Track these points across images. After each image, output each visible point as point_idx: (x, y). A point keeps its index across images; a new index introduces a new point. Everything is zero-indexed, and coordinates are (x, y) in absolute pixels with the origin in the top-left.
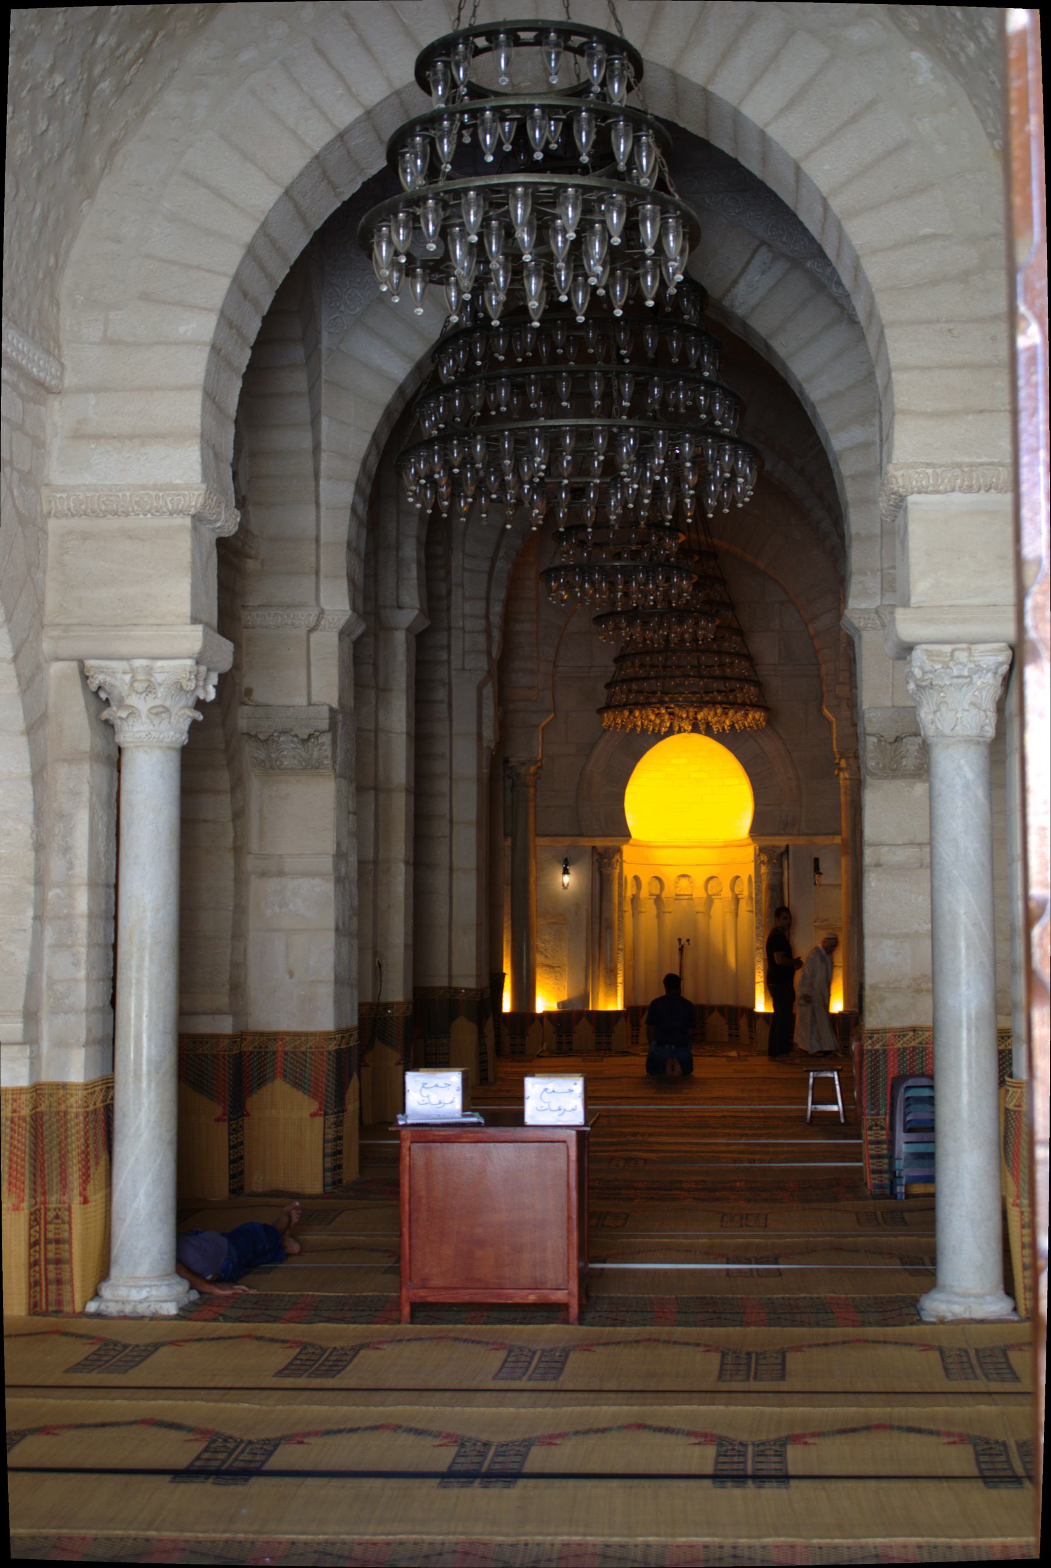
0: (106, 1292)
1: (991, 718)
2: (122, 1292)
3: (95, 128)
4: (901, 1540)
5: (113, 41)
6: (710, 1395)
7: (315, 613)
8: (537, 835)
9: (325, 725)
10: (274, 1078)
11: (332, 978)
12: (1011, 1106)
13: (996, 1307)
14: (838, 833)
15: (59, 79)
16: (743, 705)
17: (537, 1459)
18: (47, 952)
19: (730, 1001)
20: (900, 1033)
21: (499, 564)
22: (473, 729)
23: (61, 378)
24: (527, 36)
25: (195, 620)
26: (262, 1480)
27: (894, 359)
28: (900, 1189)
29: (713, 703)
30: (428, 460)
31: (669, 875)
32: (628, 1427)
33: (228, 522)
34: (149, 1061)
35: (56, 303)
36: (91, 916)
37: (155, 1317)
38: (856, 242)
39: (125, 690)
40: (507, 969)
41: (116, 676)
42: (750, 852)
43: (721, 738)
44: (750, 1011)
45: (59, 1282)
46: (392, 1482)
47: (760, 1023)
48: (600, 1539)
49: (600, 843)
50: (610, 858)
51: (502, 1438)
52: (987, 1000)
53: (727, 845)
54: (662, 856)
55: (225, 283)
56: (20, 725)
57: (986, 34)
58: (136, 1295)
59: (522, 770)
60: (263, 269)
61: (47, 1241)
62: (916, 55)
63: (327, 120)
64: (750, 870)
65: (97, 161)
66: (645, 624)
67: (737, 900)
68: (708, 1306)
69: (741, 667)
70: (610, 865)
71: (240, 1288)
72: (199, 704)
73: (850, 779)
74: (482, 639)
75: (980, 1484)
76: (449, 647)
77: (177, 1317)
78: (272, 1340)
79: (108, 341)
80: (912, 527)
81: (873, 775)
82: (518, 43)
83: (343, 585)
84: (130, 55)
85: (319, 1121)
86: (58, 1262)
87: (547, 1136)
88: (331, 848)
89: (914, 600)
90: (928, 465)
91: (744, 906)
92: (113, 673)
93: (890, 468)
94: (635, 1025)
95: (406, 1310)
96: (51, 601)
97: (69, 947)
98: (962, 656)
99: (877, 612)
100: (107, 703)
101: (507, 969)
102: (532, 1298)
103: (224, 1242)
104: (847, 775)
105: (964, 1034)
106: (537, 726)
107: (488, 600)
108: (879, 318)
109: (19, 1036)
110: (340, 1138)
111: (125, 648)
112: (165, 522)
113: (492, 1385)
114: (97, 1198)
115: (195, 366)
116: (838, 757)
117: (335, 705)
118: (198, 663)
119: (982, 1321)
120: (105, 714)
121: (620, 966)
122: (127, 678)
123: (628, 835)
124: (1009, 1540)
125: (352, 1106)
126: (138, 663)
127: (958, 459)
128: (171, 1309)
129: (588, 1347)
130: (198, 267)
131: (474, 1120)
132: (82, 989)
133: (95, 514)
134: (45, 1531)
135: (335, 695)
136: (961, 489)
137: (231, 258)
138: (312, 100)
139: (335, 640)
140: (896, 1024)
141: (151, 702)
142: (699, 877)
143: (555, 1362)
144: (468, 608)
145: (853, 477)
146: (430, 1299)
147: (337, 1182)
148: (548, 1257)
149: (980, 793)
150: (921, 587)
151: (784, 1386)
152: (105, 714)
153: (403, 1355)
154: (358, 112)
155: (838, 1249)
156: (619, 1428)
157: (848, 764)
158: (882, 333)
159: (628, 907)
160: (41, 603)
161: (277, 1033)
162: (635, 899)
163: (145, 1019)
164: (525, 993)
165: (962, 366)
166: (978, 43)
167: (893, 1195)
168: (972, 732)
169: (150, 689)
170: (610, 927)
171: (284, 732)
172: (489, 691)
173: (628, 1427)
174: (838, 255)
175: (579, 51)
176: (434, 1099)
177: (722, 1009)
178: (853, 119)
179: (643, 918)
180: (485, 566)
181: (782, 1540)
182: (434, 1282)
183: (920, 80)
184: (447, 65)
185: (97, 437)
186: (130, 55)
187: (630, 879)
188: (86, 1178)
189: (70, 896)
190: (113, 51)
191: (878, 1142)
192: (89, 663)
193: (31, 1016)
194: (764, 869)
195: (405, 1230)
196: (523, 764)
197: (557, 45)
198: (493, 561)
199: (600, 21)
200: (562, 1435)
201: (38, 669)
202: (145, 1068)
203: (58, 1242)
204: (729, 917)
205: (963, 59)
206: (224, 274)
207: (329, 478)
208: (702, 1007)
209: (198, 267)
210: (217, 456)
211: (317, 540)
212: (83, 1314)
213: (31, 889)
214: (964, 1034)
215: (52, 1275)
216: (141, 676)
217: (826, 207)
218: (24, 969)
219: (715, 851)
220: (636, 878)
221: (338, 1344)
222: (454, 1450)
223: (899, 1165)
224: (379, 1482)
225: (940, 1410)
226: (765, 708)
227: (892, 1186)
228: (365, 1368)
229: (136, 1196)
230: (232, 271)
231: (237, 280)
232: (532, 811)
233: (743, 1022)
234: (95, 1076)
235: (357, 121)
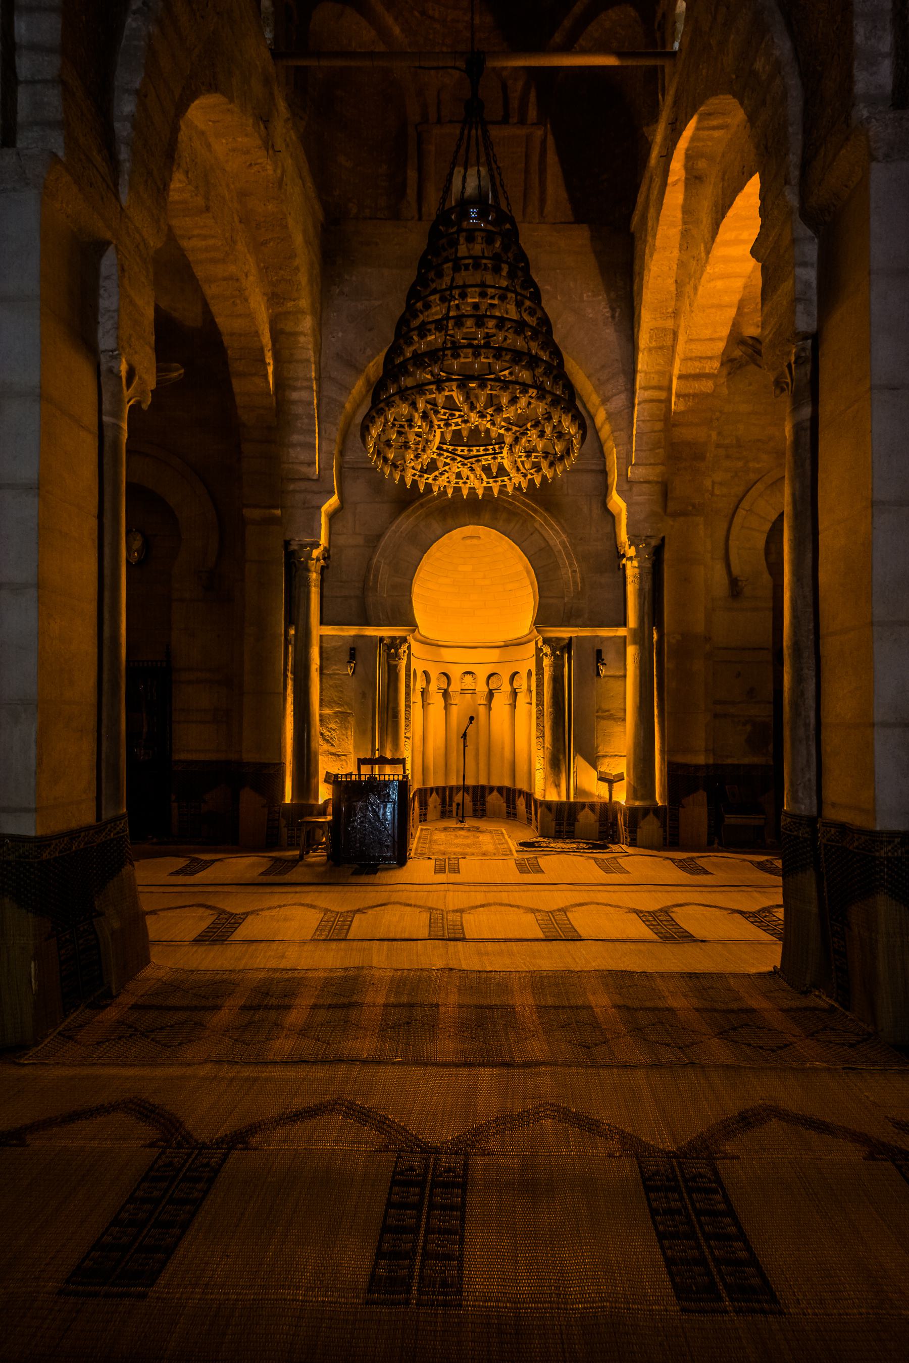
8: (322, 623)
31: (456, 672)
44: (529, 796)
49: (386, 632)
70: (397, 655)
73: (639, 567)
106: (319, 508)
177: (500, 790)
187: (419, 674)
194: (547, 662)
204: (507, 708)
219: (497, 651)
220: (425, 673)
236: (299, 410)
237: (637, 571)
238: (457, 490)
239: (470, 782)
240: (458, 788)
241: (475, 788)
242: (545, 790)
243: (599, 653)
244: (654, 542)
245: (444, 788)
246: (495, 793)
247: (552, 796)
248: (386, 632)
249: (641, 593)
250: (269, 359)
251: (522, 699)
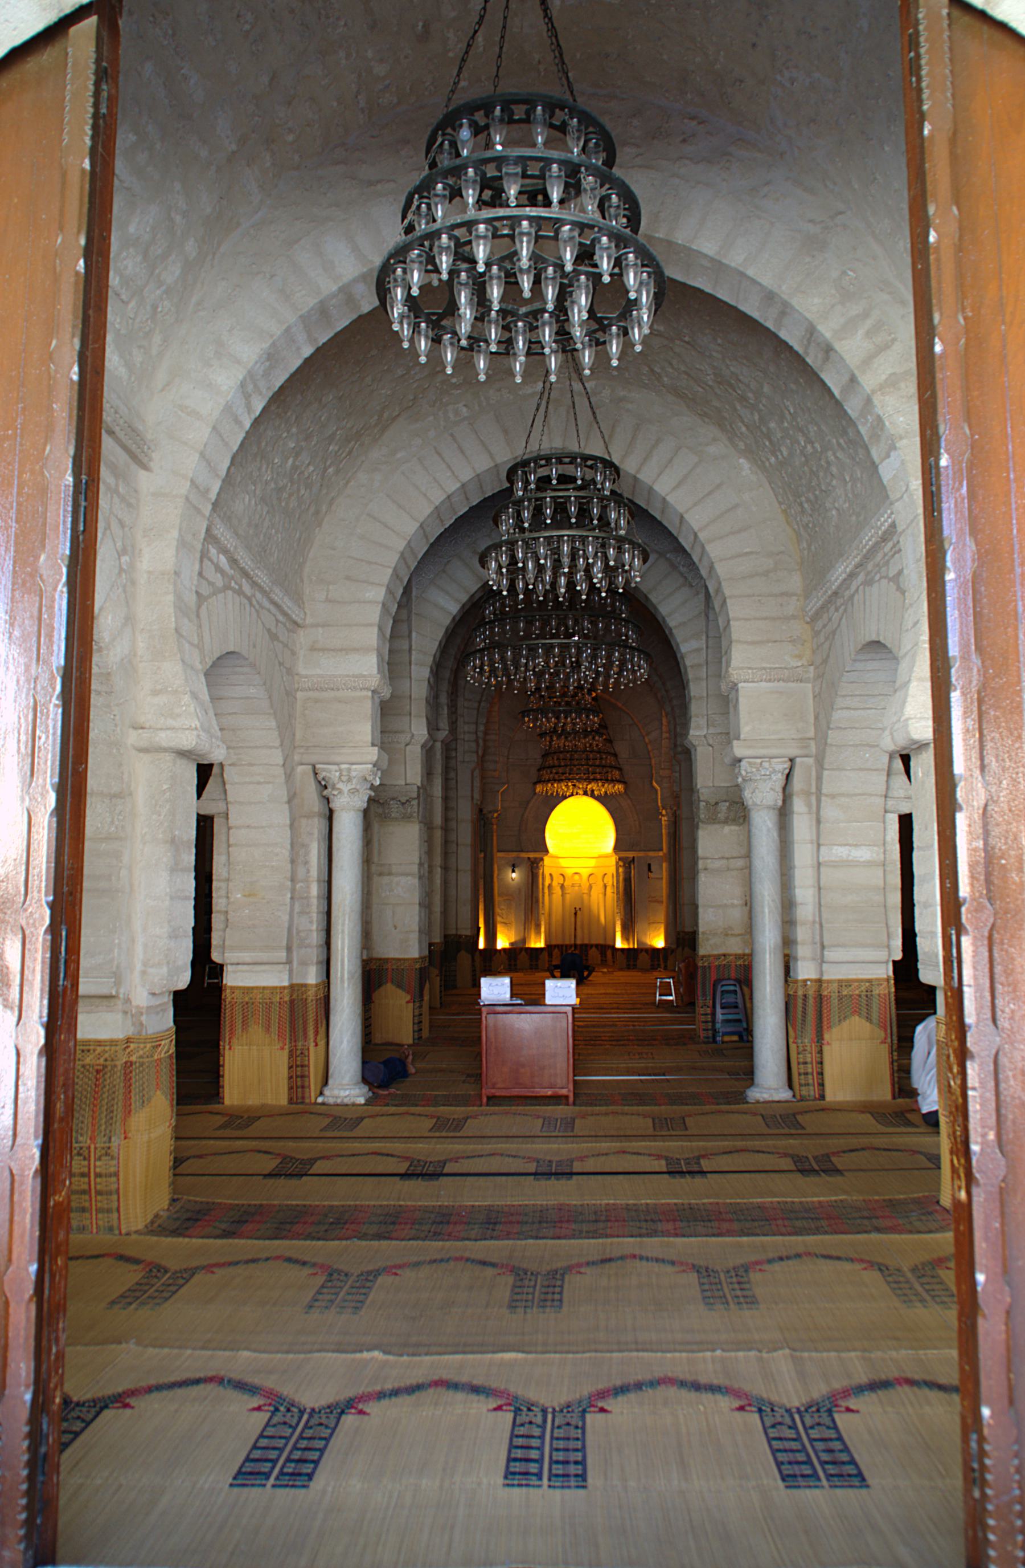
0: (327, 1092)
1: (781, 795)
2: (336, 1092)
3: (324, 491)
4: (770, 1200)
5: (337, 448)
6: (653, 1137)
7: (409, 736)
9: (415, 795)
10: (386, 982)
11: (417, 929)
12: (791, 993)
13: (785, 1095)
15: (311, 468)
16: (612, 781)
17: (577, 1167)
18: (296, 916)
19: (602, 942)
20: (717, 957)
21: (483, 704)
22: (469, 793)
23: (304, 620)
24: (567, 460)
25: (373, 745)
26: (445, 1178)
27: (731, 615)
28: (719, 1039)
29: (595, 780)
30: (482, 659)
31: (569, 872)
32: (618, 1152)
33: (386, 693)
34: (349, 972)
35: (302, 581)
36: (318, 897)
37: (354, 1105)
38: (712, 555)
39: (336, 780)
40: (481, 925)
41: (331, 773)
42: (613, 860)
43: (598, 798)
44: (614, 946)
45: (303, 1087)
46: (510, 1178)
48: (623, 1202)
49: (532, 855)
51: (558, 1158)
52: (779, 940)
53: (600, 857)
54: (563, 863)
55: (390, 571)
56: (285, 799)
57: (782, 454)
58: (343, 1093)
59: (490, 816)
60: (406, 563)
61: (297, 1066)
62: (741, 461)
63: (442, 489)
64: (613, 870)
65: (324, 508)
66: (566, 738)
67: (605, 887)
68: (635, 1096)
69: (611, 760)
70: (537, 867)
71: (392, 1090)
72: (372, 787)
74: (474, 745)
75: (799, 1175)
76: (456, 749)
77: (365, 1104)
78: (419, 1115)
79: (328, 600)
80: (742, 700)
81: (703, 822)
82: (561, 463)
83: (424, 720)
84: (344, 455)
85: (411, 1005)
86: (302, 1077)
87: (556, 1011)
88: (417, 861)
89: (742, 736)
90: (749, 668)
91: (609, 890)
92: (330, 771)
93: (730, 669)
94: (550, 955)
95: (485, 1100)
96: (299, 735)
97: (308, 913)
98: (766, 765)
99: (705, 736)
100: (326, 787)
101: (481, 925)
102: (550, 1093)
103: (382, 1066)
105: (768, 956)
107: (477, 723)
108: (723, 593)
109: (284, 960)
110: (421, 1015)
111: (338, 759)
112: (358, 694)
113: (540, 1134)
114: (322, 1043)
115: (374, 614)
117: (419, 784)
118: (374, 766)
119: (778, 1102)
120: (325, 793)
121: (543, 923)
122: (337, 774)
123: (547, 851)
124: (822, 1199)
125: (426, 998)
126: (343, 766)
127: (765, 665)
128: (362, 1101)
129: (583, 1116)
130: (376, 563)
131: (519, 1002)
132: (315, 934)
133: (322, 690)
134: (348, 1203)
135: (420, 779)
136: (765, 681)
137: (393, 559)
138: (434, 478)
139: (419, 750)
140: (715, 952)
141: (350, 786)
142: (585, 873)
143: (570, 1123)
144: (466, 728)
145: (692, 667)
146: (497, 1094)
147: (420, 1038)
148: (557, 1071)
149: (775, 834)
150: (745, 730)
151: (687, 1133)
152: (325, 793)
153: (489, 1121)
154: (458, 485)
155: (694, 1068)
156: (614, 1153)
158: (725, 601)
159: (546, 891)
160: (294, 735)
161: (388, 959)
162: (550, 886)
163: (346, 950)
164: (491, 938)
165: (766, 619)
166: (777, 457)
167: (715, 1041)
168: (771, 803)
169: (349, 780)
170: (537, 901)
171: (393, 799)
172: (477, 773)
173: (618, 1152)
174: (700, 560)
175: (591, 467)
176: (496, 992)
177: (597, 946)
178: (710, 493)
179: (554, 896)
180: (476, 705)
181: (711, 1200)
182: (498, 1086)
183: (744, 473)
184: (525, 473)
185: (323, 650)
186: (344, 455)
188: (316, 1033)
189: (308, 887)
190: (336, 452)
191: (706, 1014)
192: (318, 766)
193: (289, 949)
194: (621, 870)
195: (484, 1059)
196: (490, 812)
197: (580, 465)
198: (480, 703)
199: (598, 451)
200: (587, 1157)
201: (293, 769)
202: (346, 976)
203: (302, 1066)
204: (601, 896)
205: (767, 464)
206: (389, 567)
207: (416, 664)
208: (586, 945)
209: (376, 563)
210: (382, 659)
211: (410, 697)
212: (316, 1103)
213: (289, 883)
214: (768, 956)
215: (299, 1084)
216: (344, 773)
217: (696, 535)
218: (286, 925)
221: (456, 1117)
222: (535, 1164)
223: (718, 1026)
224: (504, 1178)
225: (770, 1142)
226: (624, 783)
227: (714, 1037)
228: (471, 1127)
229: (342, 1042)
230: (393, 565)
231: (395, 570)
232: (495, 838)
233: (609, 953)
234: (319, 980)
235: (458, 489)
239: (579, 942)
240: (571, 946)
241: (581, 945)
245: (562, 946)
246: (594, 949)
247: (626, 946)
248: (532, 855)
251: (609, 890)
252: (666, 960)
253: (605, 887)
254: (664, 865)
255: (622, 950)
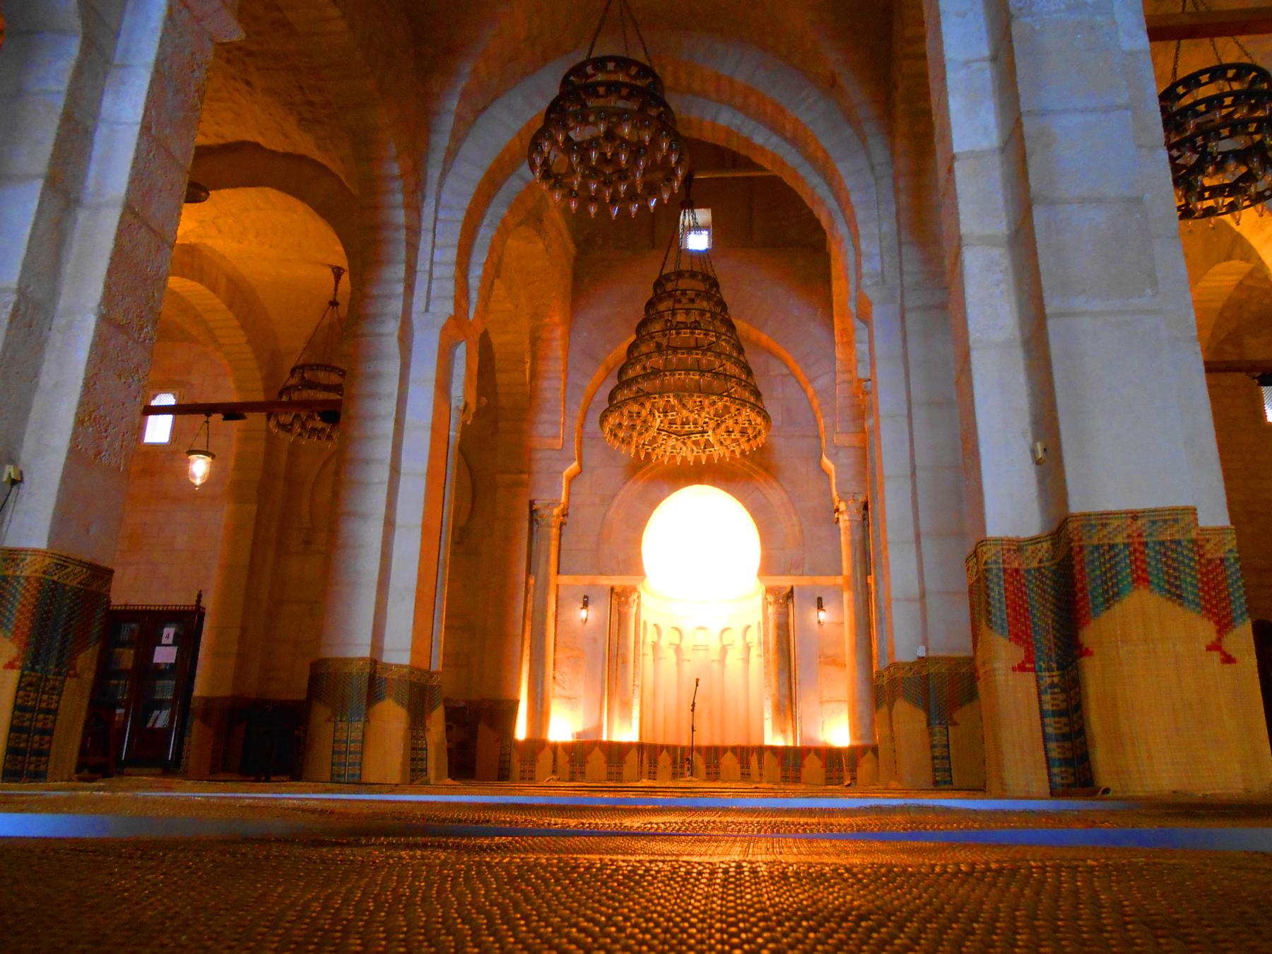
14: (841, 574)
19: (743, 743)
44: (761, 750)
47: (767, 755)
49: (617, 581)
50: (627, 598)
59: (546, 512)
64: (759, 617)
67: (748, 648)
70: (627, 603)
91: (755, 652)
104: (846, 517)
116: (837, 499)
157: (847, 507)
170: (625, 662)
177: (734, 749)
194: (771, 609)
204: (740, 664)
236: (549, 395)
237: (848, 524)
238: (673, 457)
239: (703, 740)
241: (708, 749)
242: (773, 738)
243: (820, 600)
244: (861, 499)
245: (675, 747)
246: (729, 754)
249: (852, 543)
250: (528, 360)
252: (854, 768)
253: (748, 648)
254: (847, 596)
255: (773, 750)
